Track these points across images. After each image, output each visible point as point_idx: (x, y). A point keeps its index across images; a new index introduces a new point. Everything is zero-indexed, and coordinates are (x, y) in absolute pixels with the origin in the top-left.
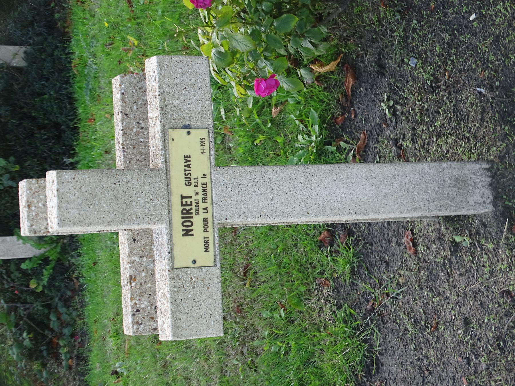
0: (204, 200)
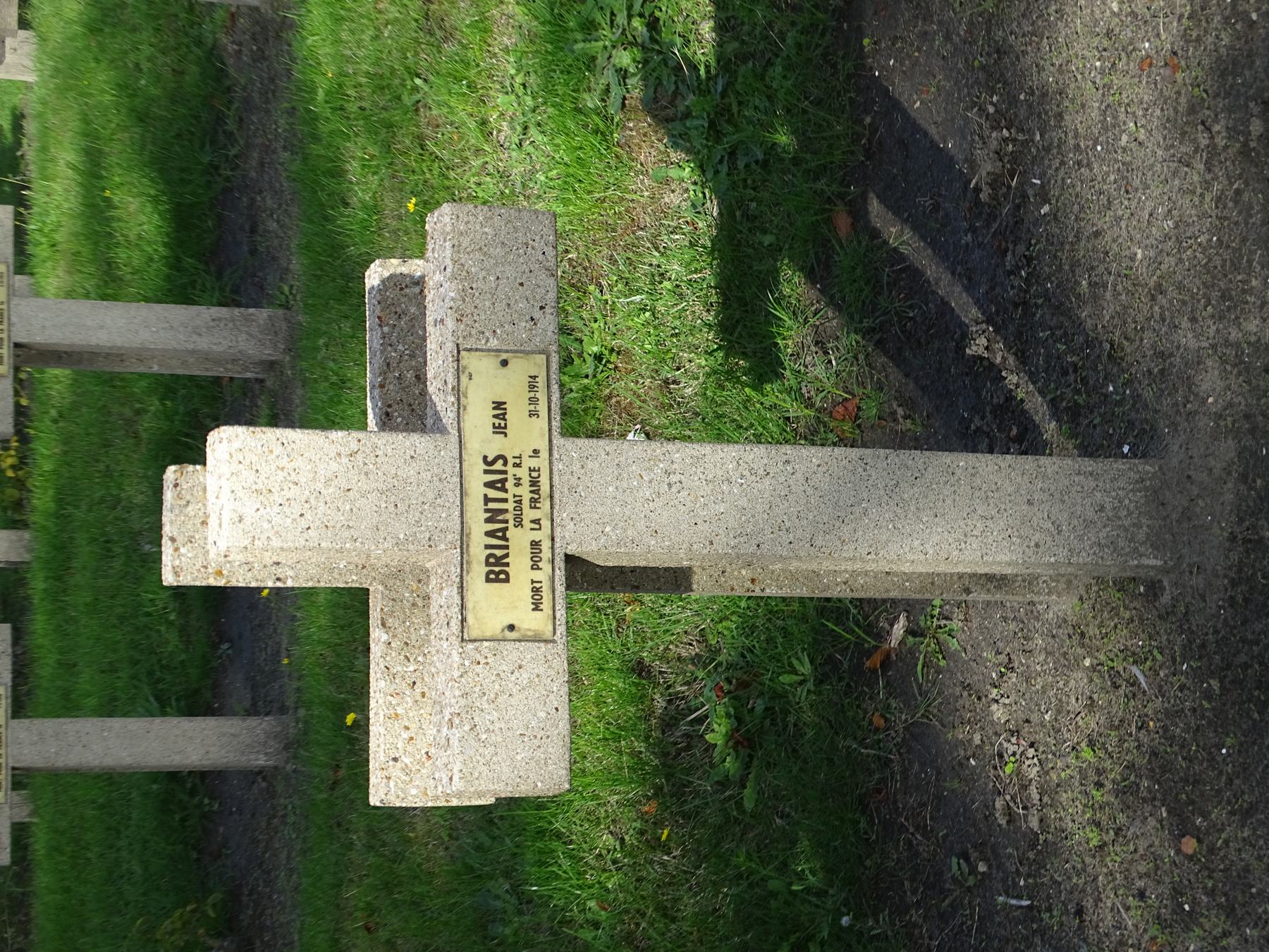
0: (534, 503)
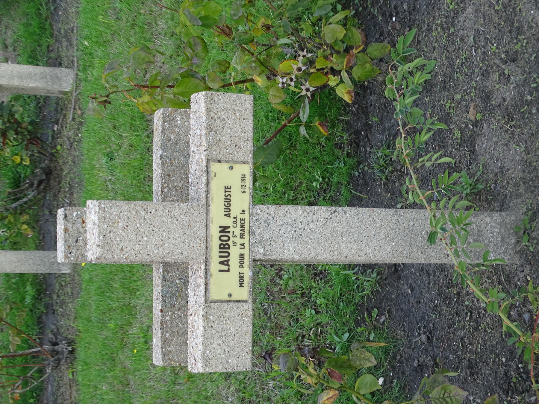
0: (242, 236)
